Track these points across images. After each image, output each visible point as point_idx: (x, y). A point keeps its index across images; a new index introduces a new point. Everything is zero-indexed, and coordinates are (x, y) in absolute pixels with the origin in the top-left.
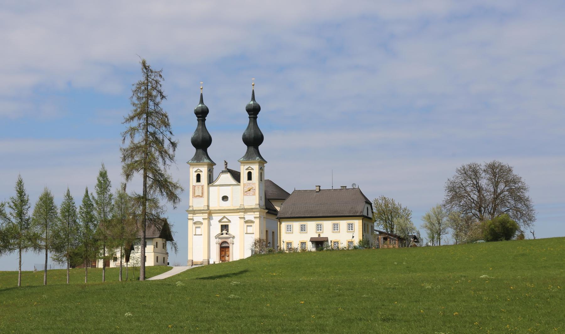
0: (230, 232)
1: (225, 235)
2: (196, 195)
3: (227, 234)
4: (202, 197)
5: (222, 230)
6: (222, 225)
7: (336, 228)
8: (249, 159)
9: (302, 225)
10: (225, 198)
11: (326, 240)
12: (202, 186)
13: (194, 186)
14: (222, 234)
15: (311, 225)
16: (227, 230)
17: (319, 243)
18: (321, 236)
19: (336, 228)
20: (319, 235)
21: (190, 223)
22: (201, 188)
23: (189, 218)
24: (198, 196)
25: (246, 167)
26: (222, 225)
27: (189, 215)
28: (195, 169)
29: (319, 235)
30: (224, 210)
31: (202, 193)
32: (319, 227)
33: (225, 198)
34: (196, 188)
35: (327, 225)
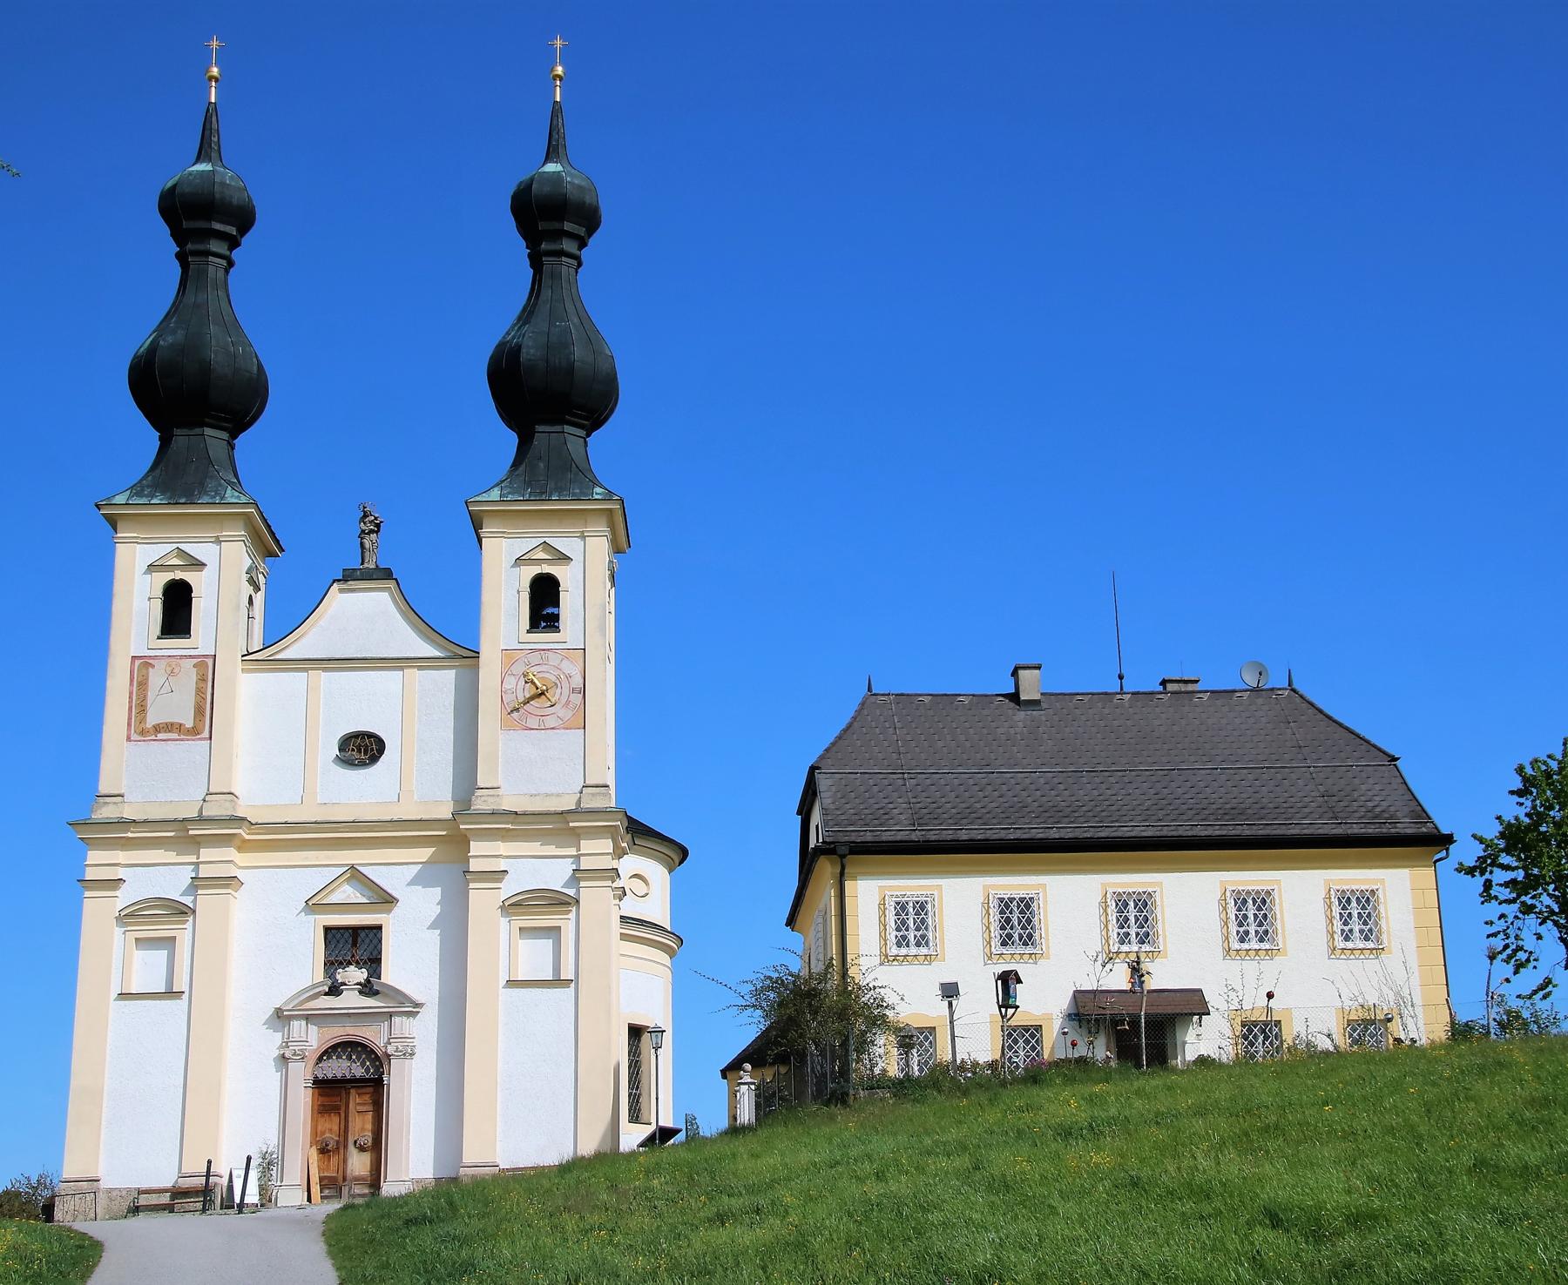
0: (391, 974)
1: (351, 1000)
2: (152, 720)
3: (367, 989)
4: (194, 732)
5: (332, 965)
6: (328, 930)
7: (1254, 921)
8: (542, 494)
9: (1005, 905)
10: (362, 749)
11: (1192, 1005)
12: (206, 669)
13: (143, 664)
14: (334, 990)
15: (1074, 905)
16: (374, 963)
17: (1137, 1030)
18: (1152, 983)
19: (1254, 921)
20: (1136, 970)
21: (98, 911)
22: (189, 677)
23: (90, 874)
24: (169, 727)
25: (522, 546)
26: (328, 930)
27: (94, 856)
28: (155, 552)
29: (1136, 970)
30: (355, 824)
31: (199, 711)
32: (1135, 917)
33: (362, 749)
34: (156, 678)
35: (1190, 898)
